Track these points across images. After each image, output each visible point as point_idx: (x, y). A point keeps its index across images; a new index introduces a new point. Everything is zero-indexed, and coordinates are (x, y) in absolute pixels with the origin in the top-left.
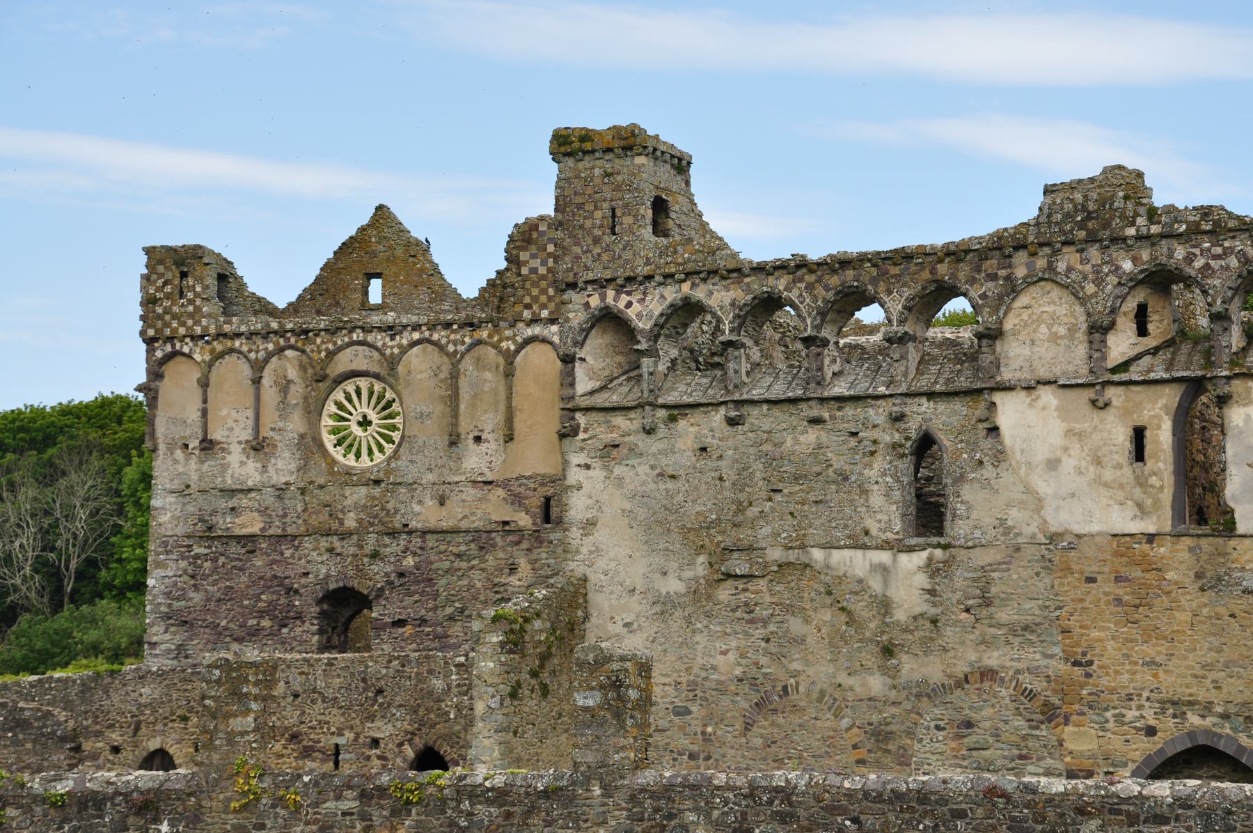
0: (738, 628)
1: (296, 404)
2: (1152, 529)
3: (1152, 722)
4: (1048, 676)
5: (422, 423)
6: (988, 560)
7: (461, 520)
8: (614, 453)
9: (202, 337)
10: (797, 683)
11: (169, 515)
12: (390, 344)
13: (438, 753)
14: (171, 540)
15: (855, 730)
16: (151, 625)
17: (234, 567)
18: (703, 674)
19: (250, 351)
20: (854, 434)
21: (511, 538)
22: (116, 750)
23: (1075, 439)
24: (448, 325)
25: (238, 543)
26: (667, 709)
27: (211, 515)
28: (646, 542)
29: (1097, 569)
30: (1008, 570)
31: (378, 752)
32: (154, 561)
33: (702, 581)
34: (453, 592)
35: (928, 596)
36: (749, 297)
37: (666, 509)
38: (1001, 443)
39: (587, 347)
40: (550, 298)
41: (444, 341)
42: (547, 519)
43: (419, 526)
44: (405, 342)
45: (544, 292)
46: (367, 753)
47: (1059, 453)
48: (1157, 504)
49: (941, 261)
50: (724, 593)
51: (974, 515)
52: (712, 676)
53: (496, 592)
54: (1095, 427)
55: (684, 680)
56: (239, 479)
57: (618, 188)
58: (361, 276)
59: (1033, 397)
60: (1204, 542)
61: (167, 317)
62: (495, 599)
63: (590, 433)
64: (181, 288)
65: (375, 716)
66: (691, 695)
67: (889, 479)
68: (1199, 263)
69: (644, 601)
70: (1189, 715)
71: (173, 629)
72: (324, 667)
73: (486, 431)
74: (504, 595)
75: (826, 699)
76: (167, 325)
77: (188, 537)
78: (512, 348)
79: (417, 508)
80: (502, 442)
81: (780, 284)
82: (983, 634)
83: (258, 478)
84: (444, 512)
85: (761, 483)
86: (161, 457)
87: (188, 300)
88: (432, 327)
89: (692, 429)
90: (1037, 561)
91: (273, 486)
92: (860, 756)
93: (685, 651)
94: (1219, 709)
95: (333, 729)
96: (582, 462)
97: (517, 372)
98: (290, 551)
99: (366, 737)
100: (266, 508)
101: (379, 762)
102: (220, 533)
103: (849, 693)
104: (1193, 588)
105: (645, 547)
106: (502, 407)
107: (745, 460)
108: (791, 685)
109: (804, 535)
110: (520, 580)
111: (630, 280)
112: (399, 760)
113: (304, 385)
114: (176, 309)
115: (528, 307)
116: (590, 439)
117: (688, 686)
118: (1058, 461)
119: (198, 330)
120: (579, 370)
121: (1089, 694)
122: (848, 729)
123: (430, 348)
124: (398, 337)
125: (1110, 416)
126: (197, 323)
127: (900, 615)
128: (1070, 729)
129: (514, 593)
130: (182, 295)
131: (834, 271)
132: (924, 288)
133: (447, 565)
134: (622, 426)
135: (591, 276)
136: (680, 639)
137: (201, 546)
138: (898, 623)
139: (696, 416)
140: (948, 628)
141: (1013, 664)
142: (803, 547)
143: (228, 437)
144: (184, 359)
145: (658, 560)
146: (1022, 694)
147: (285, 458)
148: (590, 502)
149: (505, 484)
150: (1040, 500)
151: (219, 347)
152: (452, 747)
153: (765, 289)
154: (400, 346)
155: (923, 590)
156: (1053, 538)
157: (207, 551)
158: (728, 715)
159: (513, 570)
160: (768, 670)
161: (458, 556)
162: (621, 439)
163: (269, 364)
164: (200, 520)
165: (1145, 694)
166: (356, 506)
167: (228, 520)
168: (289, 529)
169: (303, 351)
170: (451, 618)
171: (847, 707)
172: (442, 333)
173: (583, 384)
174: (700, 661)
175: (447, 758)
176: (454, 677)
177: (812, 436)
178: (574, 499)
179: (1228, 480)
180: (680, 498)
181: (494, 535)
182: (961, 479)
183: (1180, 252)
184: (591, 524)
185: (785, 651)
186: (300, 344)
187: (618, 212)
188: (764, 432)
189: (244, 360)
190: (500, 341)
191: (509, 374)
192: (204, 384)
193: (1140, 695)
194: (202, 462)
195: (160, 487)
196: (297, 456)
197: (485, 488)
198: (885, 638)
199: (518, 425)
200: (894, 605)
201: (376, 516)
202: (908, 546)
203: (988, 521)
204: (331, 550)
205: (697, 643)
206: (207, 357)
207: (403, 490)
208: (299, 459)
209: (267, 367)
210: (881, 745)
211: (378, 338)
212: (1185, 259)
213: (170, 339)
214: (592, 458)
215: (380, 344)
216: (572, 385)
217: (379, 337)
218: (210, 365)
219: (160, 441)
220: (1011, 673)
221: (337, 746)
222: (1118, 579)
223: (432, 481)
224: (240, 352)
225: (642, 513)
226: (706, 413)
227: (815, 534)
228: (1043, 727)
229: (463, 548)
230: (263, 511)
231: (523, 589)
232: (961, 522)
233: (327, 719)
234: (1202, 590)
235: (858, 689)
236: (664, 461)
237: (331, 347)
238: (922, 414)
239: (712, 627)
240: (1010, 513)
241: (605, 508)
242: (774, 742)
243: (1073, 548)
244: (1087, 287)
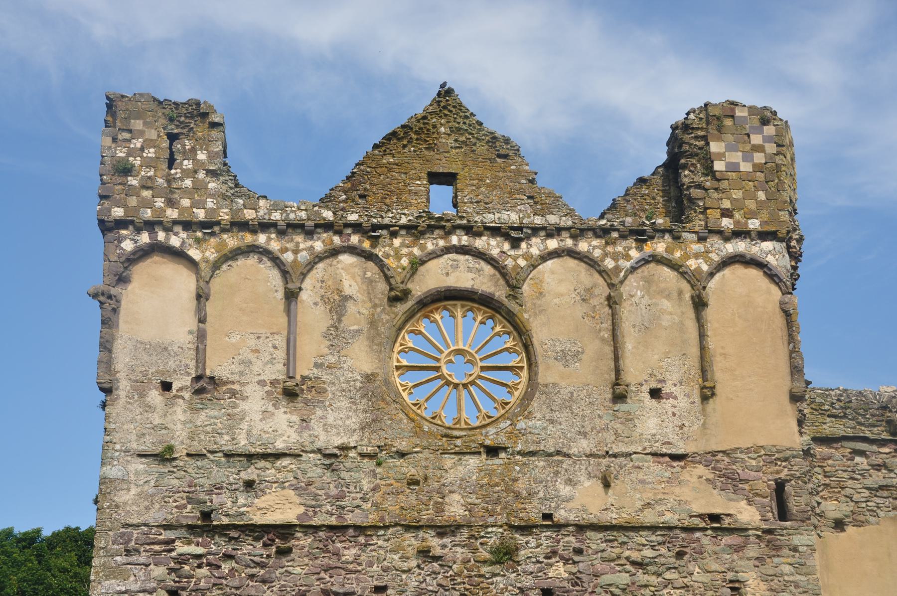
1: (357, 331)
5: (565, 366)
7: (641, 510)
9: (204, 225)
11: (134, 491)
14: (135, 533)
17: (252, 577)
19: (284, 250)
21: (727, 540)
25: (257, 539)
27: (210, 492)
32: (104, 565)
41: (597, 253)
42: (783, 514)
43: (572, 518)
44: (535, 251)
56: (260, 438)
58: (424, 175)
61: (146, 194)
64: (172, 154)
73: (669, 383)
76: (149, 204)
77: (168, 527)
78: (705, 268)
79: (565, 490)
80: (698, 400)
83: (294, 437)
84: (611, 497)
86: (123, 400)
87: (183, 171)
88: (578, 233)
91: (319, 451)
97: (712, 301)
98: (354, 551)
100: (309, 484)
102: (225, 521)
106: (695, 351)
113: (369, 305)
115: (727, 213)
119: (201, 214)
123: (571, 263)
124: (523, 245)
126: (201, 205)
130: (171, 162)
137: (189, 543)
143: (241, 374)
147: (339, 409)
151: (231, 241)
154: (527, 256)
163: (314, 272)
164: (190, 500)
166: (463, 485)
167: (241, 501)
169: (369, 256)
181: (698, 534)
186: (366, 245)
189: (269, 264)
190: (687, 257)
191: (699, 304)
192: (201, 297)
194: (195, 410)
195: (118, 447)
196: (361, 407)
197: (675, 464)
199: (720, 375)
201: (497, 501)
206: (211, 255)
209: (309, 276)
211: (494, 246)
213: (150, 226)
215: (495, 252)
217: (493, 242)
218: (216, 266)
219: (121, 375)
223: (588, 452)
229: (648, 553)
230: (303, 488)
237: (416, 251)
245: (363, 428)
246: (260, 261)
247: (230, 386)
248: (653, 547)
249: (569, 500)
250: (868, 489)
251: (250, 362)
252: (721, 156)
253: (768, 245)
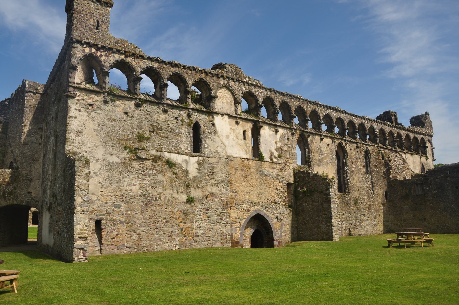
0: (140, 177)
2: (248, 158)
3: (248, 208)
4: (227, 196)
6: (213, 162)
8: (90, 107)
10: (160, 197)
15: (179, 212)
18: (126, 192)
20: (176, 118)
23: (232, 131)
26: (112, 205)
28: (104, 142)
29: (238, 167)
30: (218, 165)
33: (127, 159)
35: (198, 171)
36: (145, 66)
38: (215, 128)
47: (229, 134)
48: (249, 150)
49: (202, 73)
50: (135, 164)
51: (209, 148)
52: (130, 193)
54: (236, 129)
55: (119, 194)
57: (100, 14)
59: (223, 117)
60: (258, 162)
63: (81, 98)
66: (121, 200)
67: (187, 134)
68: (257, 93)
69: (103, 164)
70: (255, 206)
75: (170, 202)
81: (156, 65)
82: (212, 183)
85: (147, 128)
89: (122, 105)
90: (225, 163)
92: (181, 221)
93: (119, 184)
94: (261, 204)
103: (177, 200)
104: (256, 173)
105: (104, 144)
107: (142, 119)
108: (158, 197)
109: (162, 147)
111: (103, 47)
116: (81, 100)
117: (120, 196)
118: (229, 136)
121: (236, 201)
122: (176, 212)
125: (239, 126)
127: (191, 176)
128: (232, 210)
131: (172, 67)
132: (198, 80)
134: (94, 98)
135: (87, 41)
136: (117, 179)
138: (190, 178)
139: (125, 101)
140: (203, 181)
141: (219, 192)
142: (162, 151)
145: (110, 149)
146: (221, 201)
148: (80, 124)
150: (225, 146)
153: (151, 65)
155: (197, 169)
156: (229, 157)
158: (136, 207)
160: (150, 192)
162: (94, 103)
165: (247, 201)
171: (176, 205)
174: (125, 187)
177: (163, 116)
178: (73, 122)
179: (261, 147)
180: (117, 128)
182: (206, 137)
183: (254, 89)
184: (79, 133)
185: (157, 185)
187: (100, 23)
188: (148, 111)
193: (246, 201)
198: (187, 183)
200: (189, 173)
202: (193, 155)
203: (213, 150)
205: (125, 181)
210: (186, 217)
212: (255, 91)
220: (218, 194)
222: (242, 170)
225: (102, 132)
226: (127, 100)
227: (166, 147)
228: (225, 210)
232: (206, 150)
234: (258, 173)
235: (179, 199)
236: (111, 114)
238: (196, 117)
239: (130, 176)
240: (218, 148)
241: (86, 127)
242: (152, 217)
243: (232, 160)
244: (236, 92)
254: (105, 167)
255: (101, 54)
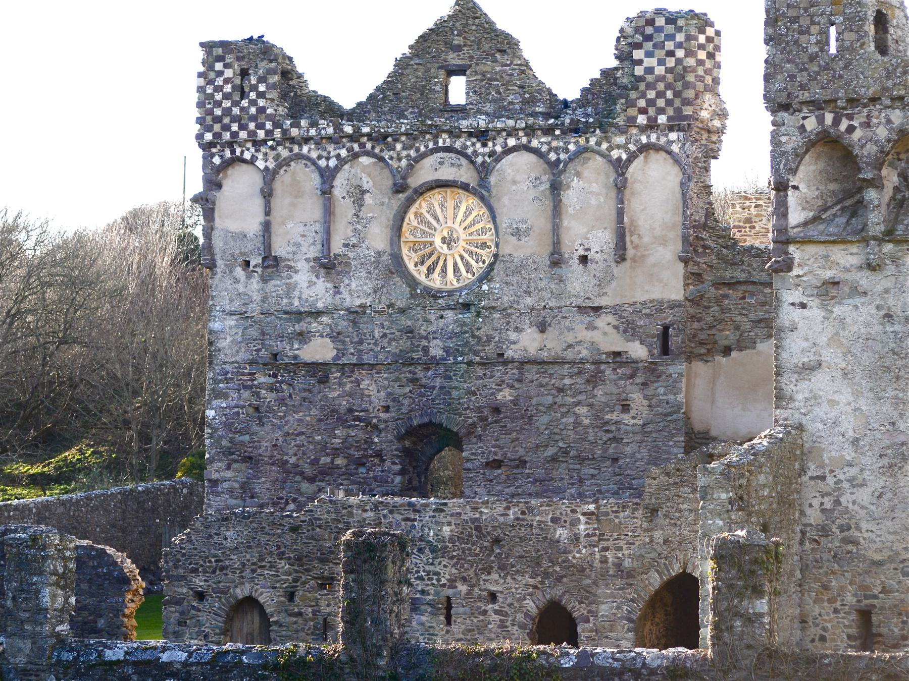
8: (833, 292)
9: (264, 142)
11: (229, 339)
12: (481, 150)
13: (565, 609)
16: (212, 460)
22: (201, 596)
24: (548, 131)
31: (496, 607)
34: (556, 430)
37: (894, 353)
39: (801, 174)
40: (669, 103)
41: (544, 148)
42: (665, 350)
45: (661, 95)
46: (484, 608)
53: (607, 431)
56: (307, 301)
61: (226, 120)
62: (605, 439)
65: (492, 568)
71: (235, 466)
72: (432, 514)
73: (593, 251)
74: (616, 434)
76: (226, 128)
78: (624, 157)
79: (513, 336)
83: (330, 300)
88: (530, 131)
91: (347, 309)
95: (443, 581)
96: (797, 301)
99: (481, 590)
100: (339, 334)
101: (497, 618)
106: (613, 225)
110: (634, 418)
112: (520, 617)
114: (236, 111)
115: (643, 111)
120: (792, 197)
129: (626, 432)
133: (550, 400)
135: (806, 96)
143: (294, 253)
144: (244, 167)
148: (805, 345)
149: (616, 310)
152: (580, 603)
157: (272, 380)
159: (626, 408)
161: (561, 390)
167: (296, 346)
168: (365, 357)
170: (554, 459)
172: (543, 140)
173: (796, 216)
175: (575, 615)
176: (582, 527)
178: (788, 341)
181: (603, 367)
189: (313, 168)
190: (610, 149)
192: (267, 194)
195: (218, 308)
196: (374, 276)
204: (414, 381)
207: (497, 315)
208: (377, 279)
214: (807, 296)
215: (470, 151)
216: (785, 215)
219: (217, 257)
221: (449, 599)
224: (308, 159)
229: (567, 381)
230: (336, 336)
231: (637, 429)
233: (437, 569)
245: (375, 292)
246: (306, 165)
247: (287, 263)
248: (571, 377)
249: (514, 343)
250: (753, 321)
251: (300, 244)
252: (640, 62)
253: (673, 136)
254: (874, 460)
255: (851, 123)
